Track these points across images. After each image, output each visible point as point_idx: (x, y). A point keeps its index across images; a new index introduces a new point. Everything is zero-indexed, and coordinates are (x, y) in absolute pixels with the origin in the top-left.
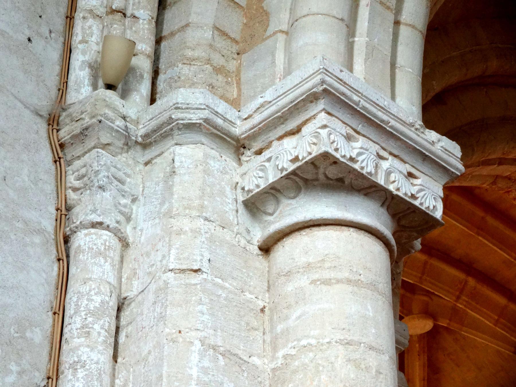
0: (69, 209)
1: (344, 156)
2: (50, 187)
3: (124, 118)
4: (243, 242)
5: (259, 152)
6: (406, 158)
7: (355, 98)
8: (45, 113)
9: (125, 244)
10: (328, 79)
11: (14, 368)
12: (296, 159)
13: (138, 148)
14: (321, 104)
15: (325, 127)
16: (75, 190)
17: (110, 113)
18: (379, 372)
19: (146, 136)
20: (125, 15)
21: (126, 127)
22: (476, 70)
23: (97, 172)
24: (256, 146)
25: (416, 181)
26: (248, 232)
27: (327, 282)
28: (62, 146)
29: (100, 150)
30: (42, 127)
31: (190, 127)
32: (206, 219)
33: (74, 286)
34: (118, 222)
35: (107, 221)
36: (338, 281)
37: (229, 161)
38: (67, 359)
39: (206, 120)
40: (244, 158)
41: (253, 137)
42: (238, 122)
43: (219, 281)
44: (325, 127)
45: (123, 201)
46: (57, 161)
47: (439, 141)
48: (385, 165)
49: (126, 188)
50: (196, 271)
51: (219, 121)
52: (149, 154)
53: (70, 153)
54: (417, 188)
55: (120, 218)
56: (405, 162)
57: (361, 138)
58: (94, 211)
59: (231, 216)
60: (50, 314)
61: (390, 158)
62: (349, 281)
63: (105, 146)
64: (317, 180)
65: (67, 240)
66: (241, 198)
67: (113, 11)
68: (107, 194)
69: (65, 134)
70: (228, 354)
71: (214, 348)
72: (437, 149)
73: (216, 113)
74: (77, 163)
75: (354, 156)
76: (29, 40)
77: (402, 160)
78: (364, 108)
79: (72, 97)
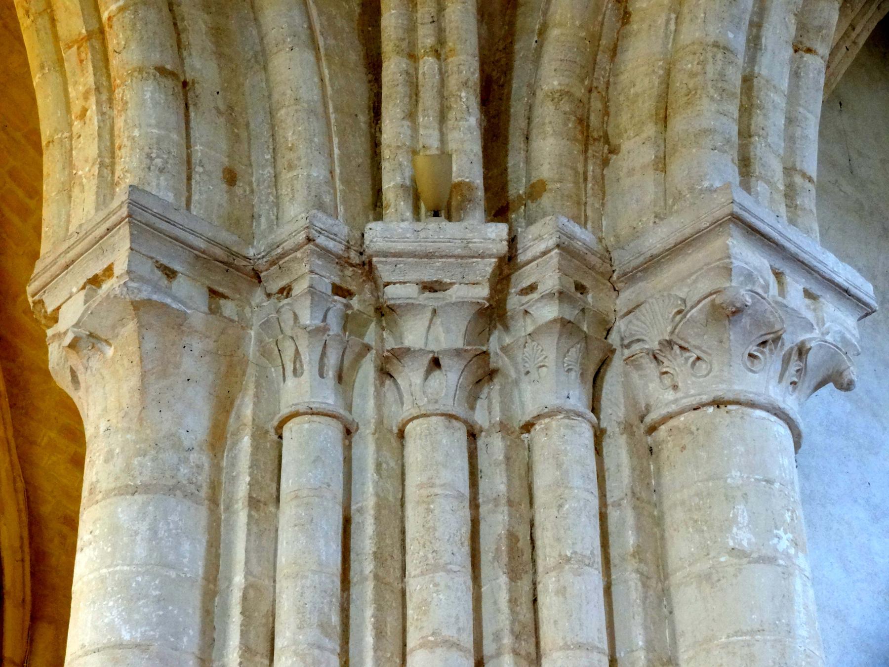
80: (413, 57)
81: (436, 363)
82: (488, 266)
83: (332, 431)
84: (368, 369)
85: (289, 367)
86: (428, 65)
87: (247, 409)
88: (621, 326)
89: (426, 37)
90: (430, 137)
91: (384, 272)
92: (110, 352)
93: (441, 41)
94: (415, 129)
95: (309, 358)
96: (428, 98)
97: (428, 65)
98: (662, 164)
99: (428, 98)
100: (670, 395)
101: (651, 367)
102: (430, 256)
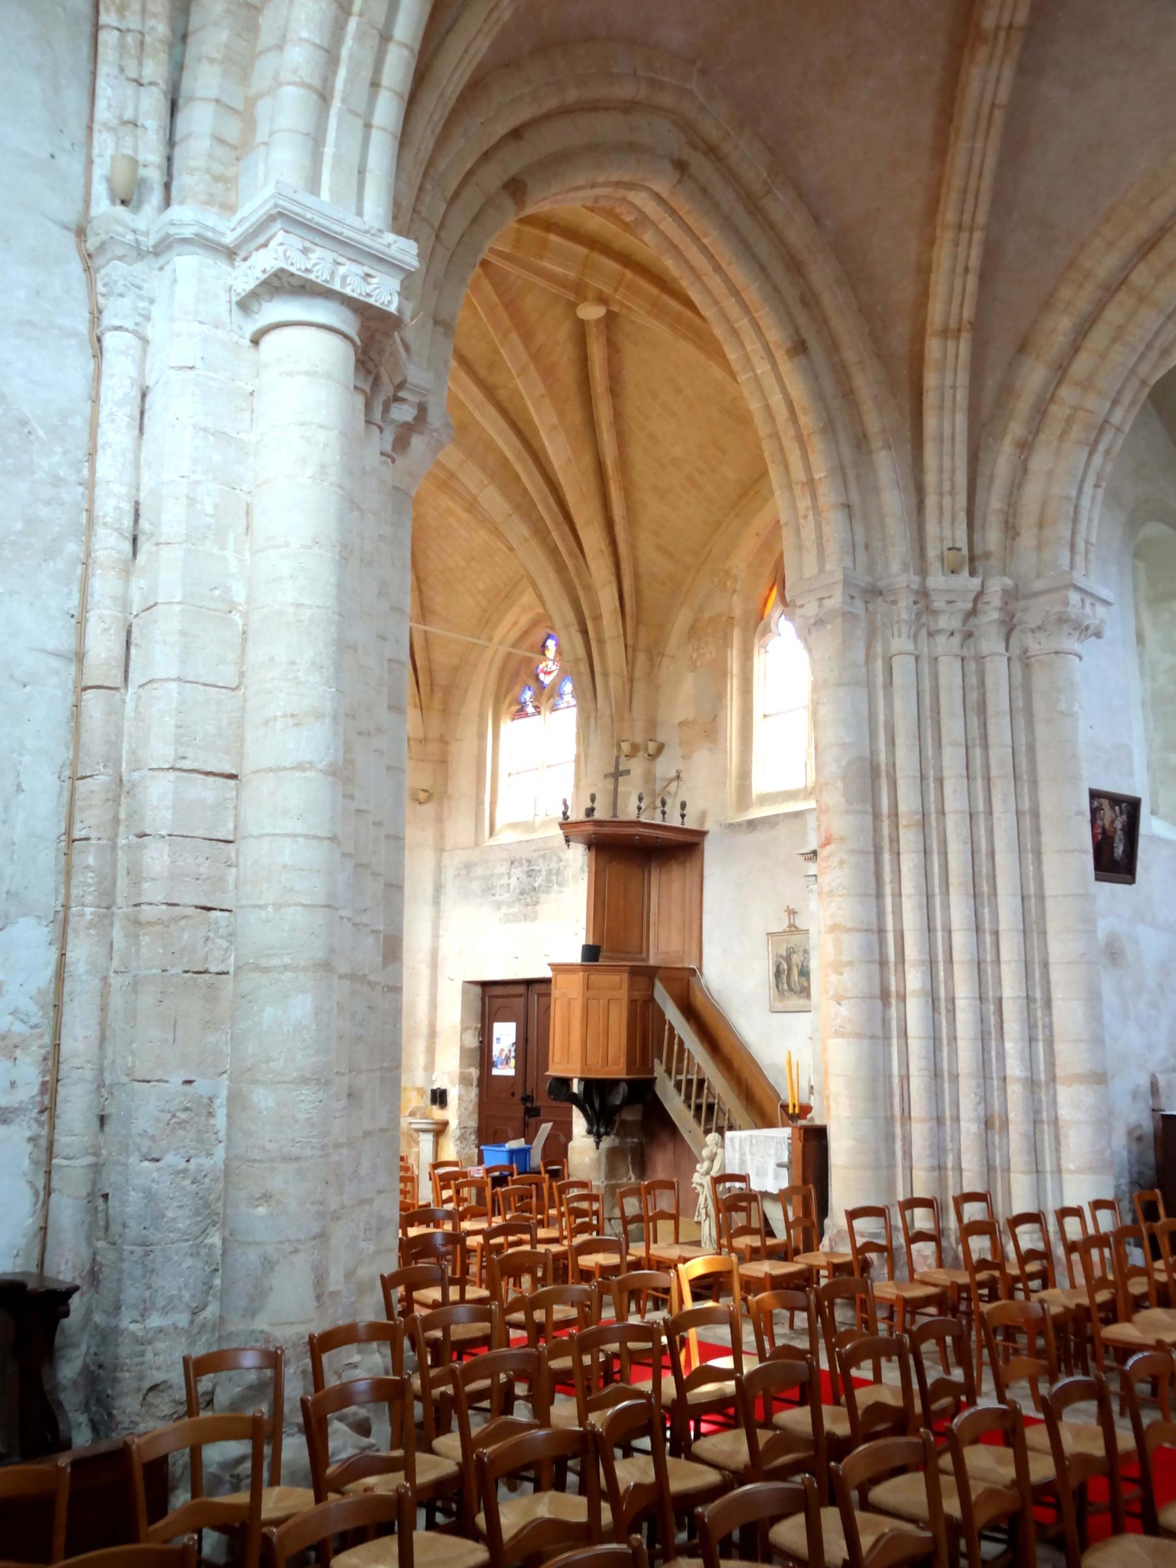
0: (100, 312)
1: (299, 269)
2: (81, 292)
3: (134, 232)
4: (235, 338)
5: (245, 259)
6: (363, 260)
7: (309, 216)
8: (73, 226)
9: (145, 341)
10: (281, 202)
11: (58, 449)
12: (264, 271)
13: (151, 256)
14: (278, 224)
15: (281, 244)
16: (103, 295)
17: (120, 229)
18: (326, 445)
19: (155, 247)
20: (136, 125)
21: (137, 241)
22: (551, 103)
23: (116, 282)
24: (242, 254)
25: (373, 281)
26: (240, 328)
27: (290, 374)
28: (89, 255)
29: (116, 262)
30: (71, 239)
31: (184, 241)
32: (201, 322)
33: (105, 381)
34: (136, 324)
35: (126, 325)
36: (299, 373)
37: (223, 266)
38: (101, 441)
39: (197, 235)
40: (236, 264)
41: (239, 246)
42: (228, 232)
43: (212, 374)
44: (281, 244)
45: (142, 304)
46: (87, 269)
48: (342, 270)
49: (144, 293)
50: (191, 368)
51: (209, 234)
52: (161, 261)
53: (99, 261)
54: (372, 287)
55: (138, 319)
56: (363, 264)
57: (318, 249)
58: (115, 316)
59: (225, 317)
60: (89, 402)
61: (348, 263)
62: (307, 373)
63: (120, 258)
64: (283, 287)
65: (99, 340)
66: (235, 299)
67: (125, 123)
68: (125, 300)
69: (92, 243)
70: (218, 433)
71: (205, 430)
72: (393, 251)
73: (207, 227)
74: (103, 271)
75: (309, 267)
76: (52, 156)
78: (317, 224)
79: (95, 211)
80: (941, 495)
81: (952, 634)
82: (973, 595)
83: (912, 660)
84: (923, 633)
85: (896, 634)
86: (947, 500)
87: (879, 648)
88: (1018, 615)
89: (947, 486)
90: (947, 532)
91: (934, 596)
92: (829, 627)
93: (953, 487)
94: (942, 528)
95: (904, 631)
96: (947, 515)
97: (947, 500)
98: (1039, 547)
99: (947, 515)
100: (1037, 647)
101: (1030, 635)
102: (952, 591)
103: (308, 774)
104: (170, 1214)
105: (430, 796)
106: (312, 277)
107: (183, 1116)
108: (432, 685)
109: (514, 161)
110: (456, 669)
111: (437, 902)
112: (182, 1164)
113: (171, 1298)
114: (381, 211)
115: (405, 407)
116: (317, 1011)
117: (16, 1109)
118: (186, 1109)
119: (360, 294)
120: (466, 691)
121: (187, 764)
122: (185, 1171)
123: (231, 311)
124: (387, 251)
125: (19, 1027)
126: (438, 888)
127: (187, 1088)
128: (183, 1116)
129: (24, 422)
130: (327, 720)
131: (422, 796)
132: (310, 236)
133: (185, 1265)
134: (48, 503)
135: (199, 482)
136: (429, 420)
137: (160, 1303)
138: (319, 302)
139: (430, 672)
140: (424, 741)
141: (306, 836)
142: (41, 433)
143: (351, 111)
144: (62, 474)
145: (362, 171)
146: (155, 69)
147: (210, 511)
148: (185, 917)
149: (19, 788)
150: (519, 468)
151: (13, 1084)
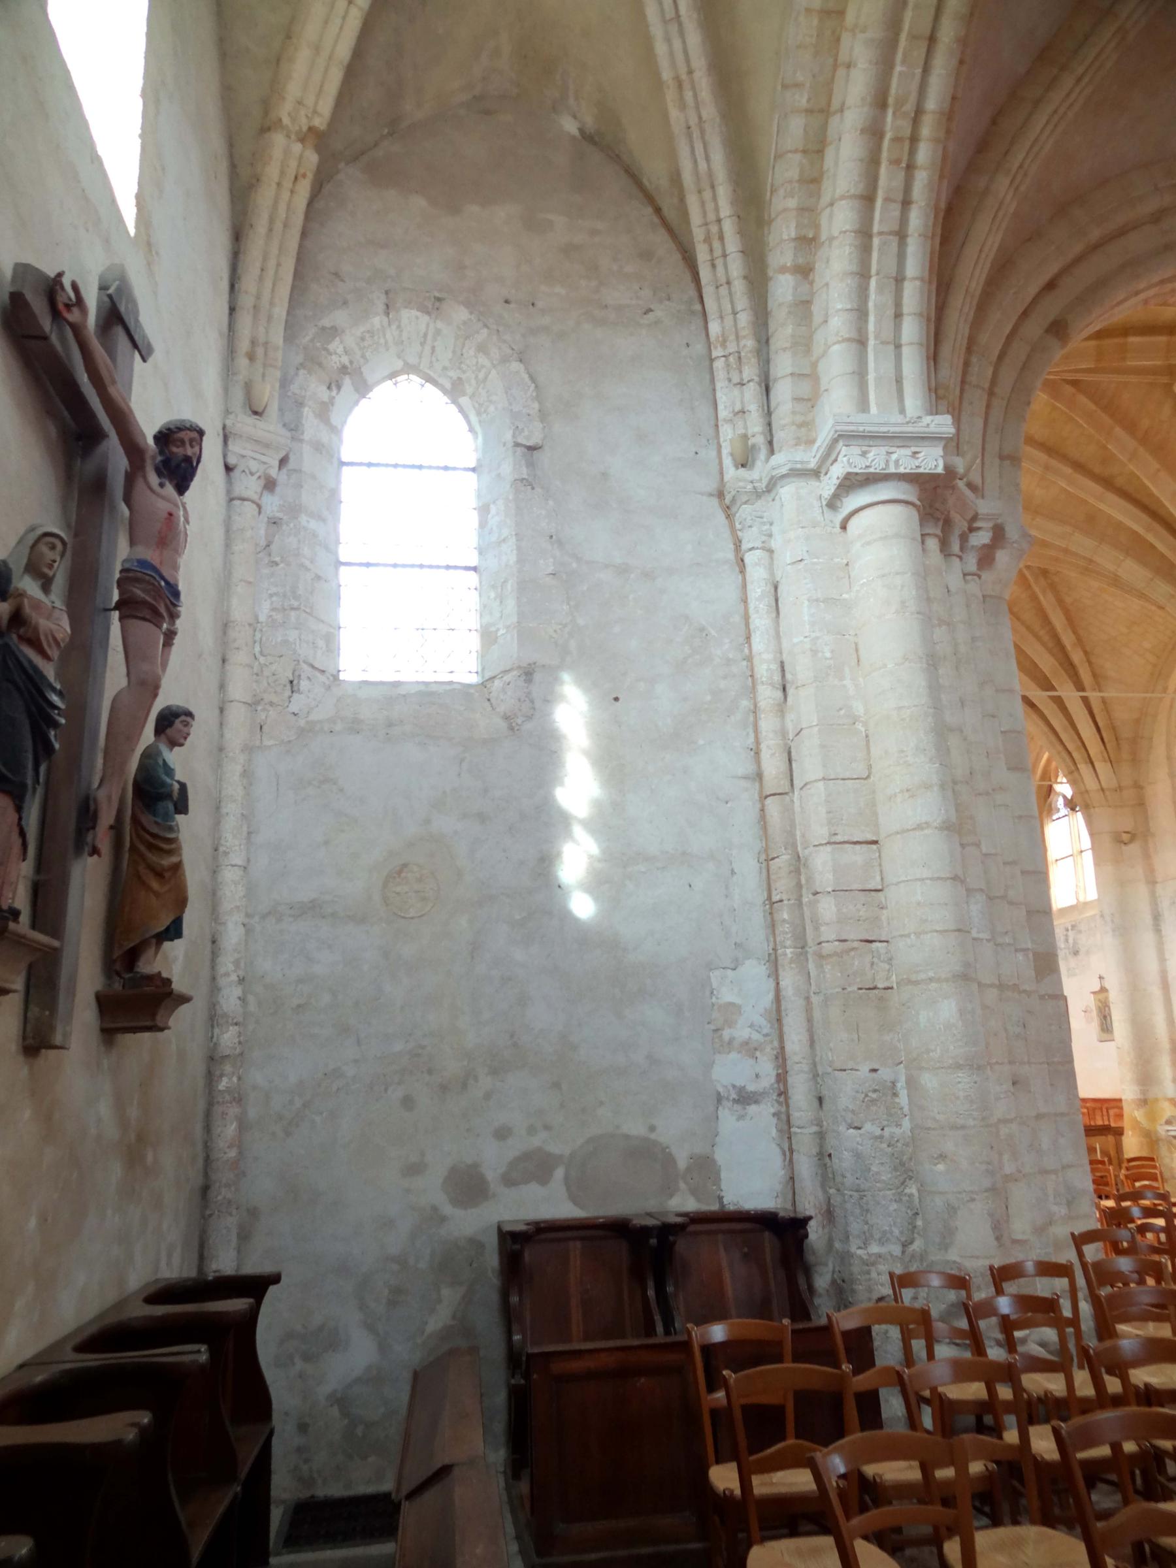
0: (740, 542)
1: (861, 468)
2: (727, 534)
3: (752, 482)
4: (829, 529)
5: (826, 474)
7: (861, 429)
8: (715, 493)
9: (771, 551)
10: (838, 428)
11: (727, 641)
12: (838, 478)
13: (766, 494)
14: (841, 443)
15: (845, 456)
16: (740, 530)
17: (741, 484)
18: (903, 586)
19: (767, 487)
20: (744, 412)
21: (754, 488)
22: (1078, 248)
23: (745, 519)
24: (823, 471)
26: (831, 521)
27: (868, 543)
28: (728, 507)
30: (715, 501)
31: (784, 476)
32: (802, 527)
33: (749, 587)
34: (763, 542)
35: (756, 546)
36: (875, 540)
37: (813, 483)
38: (752, 627)
39: (790, 470)
40: (821, 479)
41: (820, 467)
42: (812, 460)
43: (815, 560)
44: (845, 456)
45: (766, 527)
46: (728, 517)
47: (932, 421)
48: (894, 457)
49: (765, 520)
50: (801, 561)
51: (799, 466)
52: (773, 494)
53: (734, 509)
54: (920, 460)
55: (764, 538)
58: (749, 542)
59: (820, 518)
60: (742, 603)
61: (898, 450)
62: (881, 539)
63: (745, 503)
64: (854, 484)
65: (742, 560)
66: (824, 503)
67: (736, 414)
68: (754, 529)
69: (727, 501)
70: (826, 600)
71: (817, 600)
72: (932, 428)
73: (796, 462)
74: (737, 515)
75: (868, 464)
76: (696, 453)
77: (908, 447)
79: (727, 478)
103: (926, 831)
104: (874, 1169)
105: (1133, 837)
106: (872, 470)
107: (874, 1096)
108: (1117, 739)
109: (1052, 307)
110: (1137, 721)
111: (1158, 930)
112: (878, 1132)
113: (885, 1232)
114: (919, 403)
115: (981, 533)
116: (962, 1012)
117: (763, 1093)
118: (875, 1091)
119: (911, 469)
120: (1151, 739)
121: (839, 838)
122: (881, 1137)
123: (823, 512)
124: (927, 430)
125: (756, 1036)
126: (1157, 917)
127: (874, 1075)
128: (874, 1096)
129: (702, 629)
130: (935, 789)
131: (1125, 837)
132: (866, 442)
133: (891, 1208)
134: (725, 677)
135: (817, 638)
136: (1007, 535)
137: (877, 1236)
138: (880, 485)
139: (1114, 728)
140: (1120, 788)
141: (931, 879)
142: (713, 633)
143: (882, 343)
144: (731, 656)
145: (899, 381)
146: (750, 371)
147: (828, 655)
148: (853, 949)
149: (733, 872)
150: (1150, 538)
151: (757, 1076)
